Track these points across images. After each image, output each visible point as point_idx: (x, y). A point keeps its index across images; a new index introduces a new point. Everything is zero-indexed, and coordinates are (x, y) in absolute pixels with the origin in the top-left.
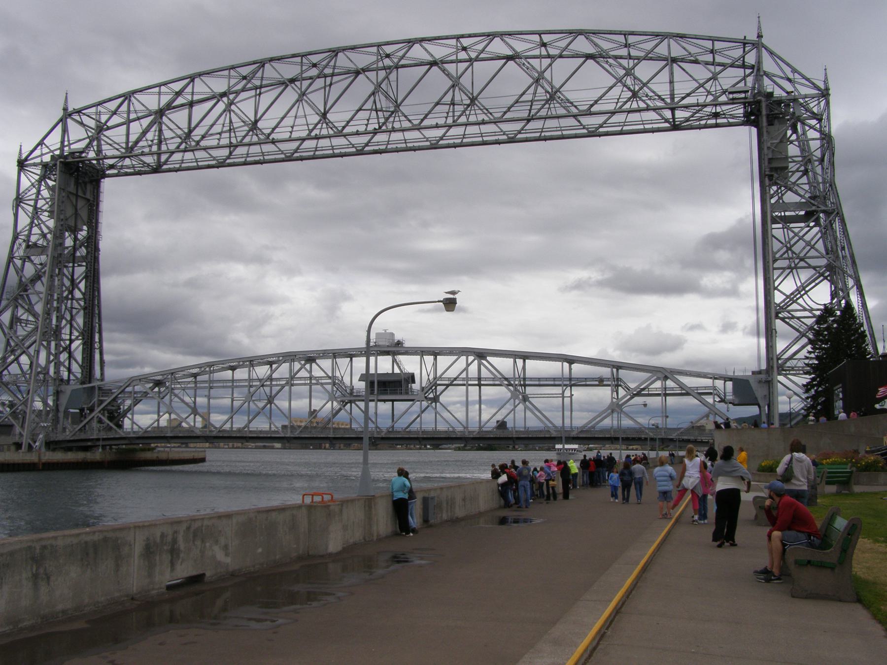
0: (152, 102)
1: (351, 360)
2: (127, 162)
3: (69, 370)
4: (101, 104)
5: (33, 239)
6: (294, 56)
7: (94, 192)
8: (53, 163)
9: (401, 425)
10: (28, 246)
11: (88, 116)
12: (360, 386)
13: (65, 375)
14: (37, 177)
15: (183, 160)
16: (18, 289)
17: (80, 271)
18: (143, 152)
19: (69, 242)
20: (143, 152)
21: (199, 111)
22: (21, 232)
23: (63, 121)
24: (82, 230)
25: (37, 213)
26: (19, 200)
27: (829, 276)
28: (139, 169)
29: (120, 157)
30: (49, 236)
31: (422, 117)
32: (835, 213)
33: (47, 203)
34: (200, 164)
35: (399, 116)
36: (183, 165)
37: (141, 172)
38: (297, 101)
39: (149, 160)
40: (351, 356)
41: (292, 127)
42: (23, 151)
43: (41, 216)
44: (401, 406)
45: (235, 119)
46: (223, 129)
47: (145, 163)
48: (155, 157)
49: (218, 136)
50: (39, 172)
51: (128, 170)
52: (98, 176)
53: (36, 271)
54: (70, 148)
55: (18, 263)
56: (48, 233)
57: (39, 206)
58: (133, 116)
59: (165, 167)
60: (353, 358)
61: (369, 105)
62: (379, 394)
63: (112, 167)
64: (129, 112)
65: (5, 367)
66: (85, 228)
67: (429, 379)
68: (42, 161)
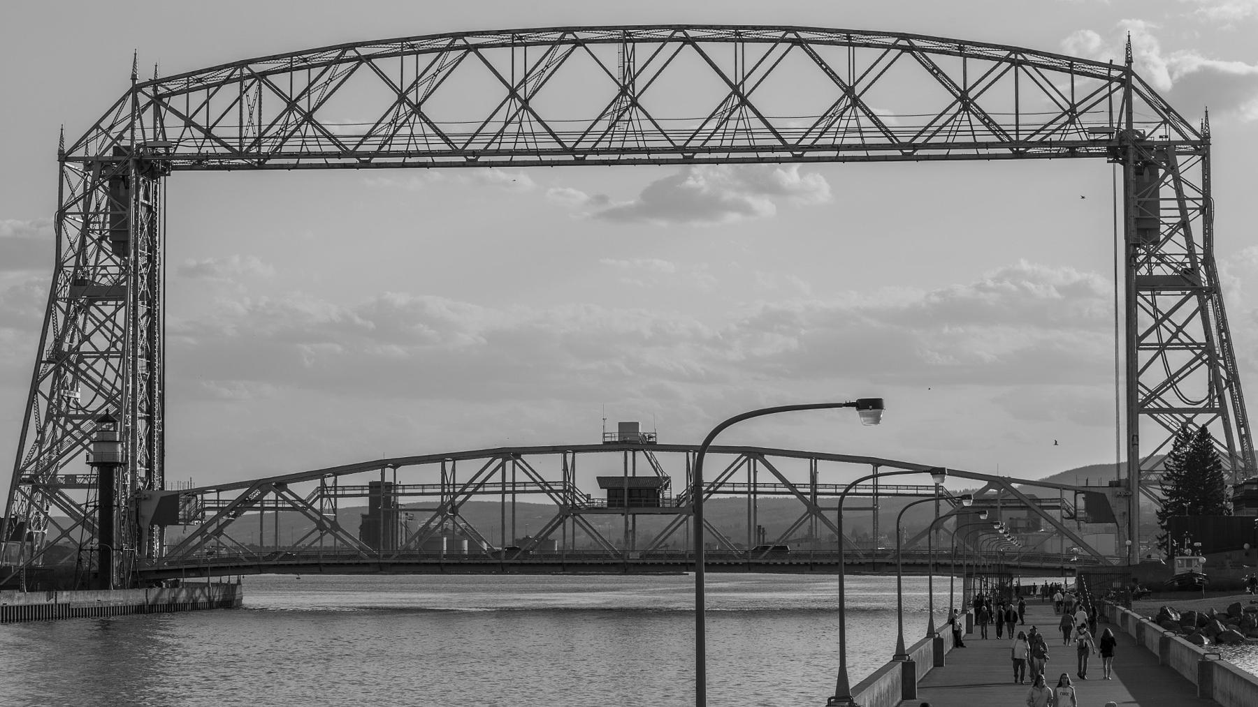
12: (600, 496)
26: (61, 214)
27: (1207, 359)
32: (1214, 290)
40: (574, 452)
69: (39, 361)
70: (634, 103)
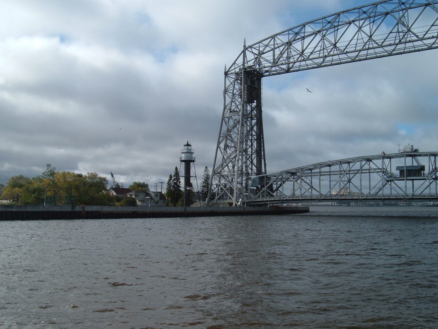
0: (285, 39)
1: (390, 160)
2: (273, 69)
3: (252, 169)
4: (261, 42)
5: (233, 108)
6: (355, 9)
7: (258, 84)
8: (240, 72)
9: (418, 192)
10: (231, 112)
11: (255, 48)
12: (397, 173)
13: (250, 171)
14: (233, 79)
15: (300, 66)
16: (227, 132)
17: (254, 122)
18: (282, 63)
19: (249, 108)
20: (282, 63)
21: (307, 41)
22: (227, 105)
23: (244, 52)
24: (254, 102)
25: (234, 96)
26: (226, 91)
28: (279, 71)
29: (272, 67)
30: (239, 107)
31: (424, 33)
33: (237, 91)
34: (309, 67)
35: (410, 34)
36: (300, 68)
37: (280, 73)
38: (358, 31)
39: (284, 67)
41: (356, 45)
42: (226, 68)
43: (236, 97)
44: (417, 183)
45: (326, 43)
46: (321, 48)
47: (282, 68)
48: (287, 65)
49: (319, 52)
50: (234, 77)
51: (274, 73)
52: (260, 76)
53: (234, 123)
54: (248, 64)
55: (227, 119)
56: (239, 105)
57: (234, 93)
58: (276, 46)
59: (291, 70)
60: (391, 159)
61: (395, 30)
62: (406, 177)
63: (267, 71)
64: (274, 44)
65: (223, 168)
66: (255, 101)
67: (433, 168)
68: (235, 71)
69: (220, 137)
70: (409, 30)
